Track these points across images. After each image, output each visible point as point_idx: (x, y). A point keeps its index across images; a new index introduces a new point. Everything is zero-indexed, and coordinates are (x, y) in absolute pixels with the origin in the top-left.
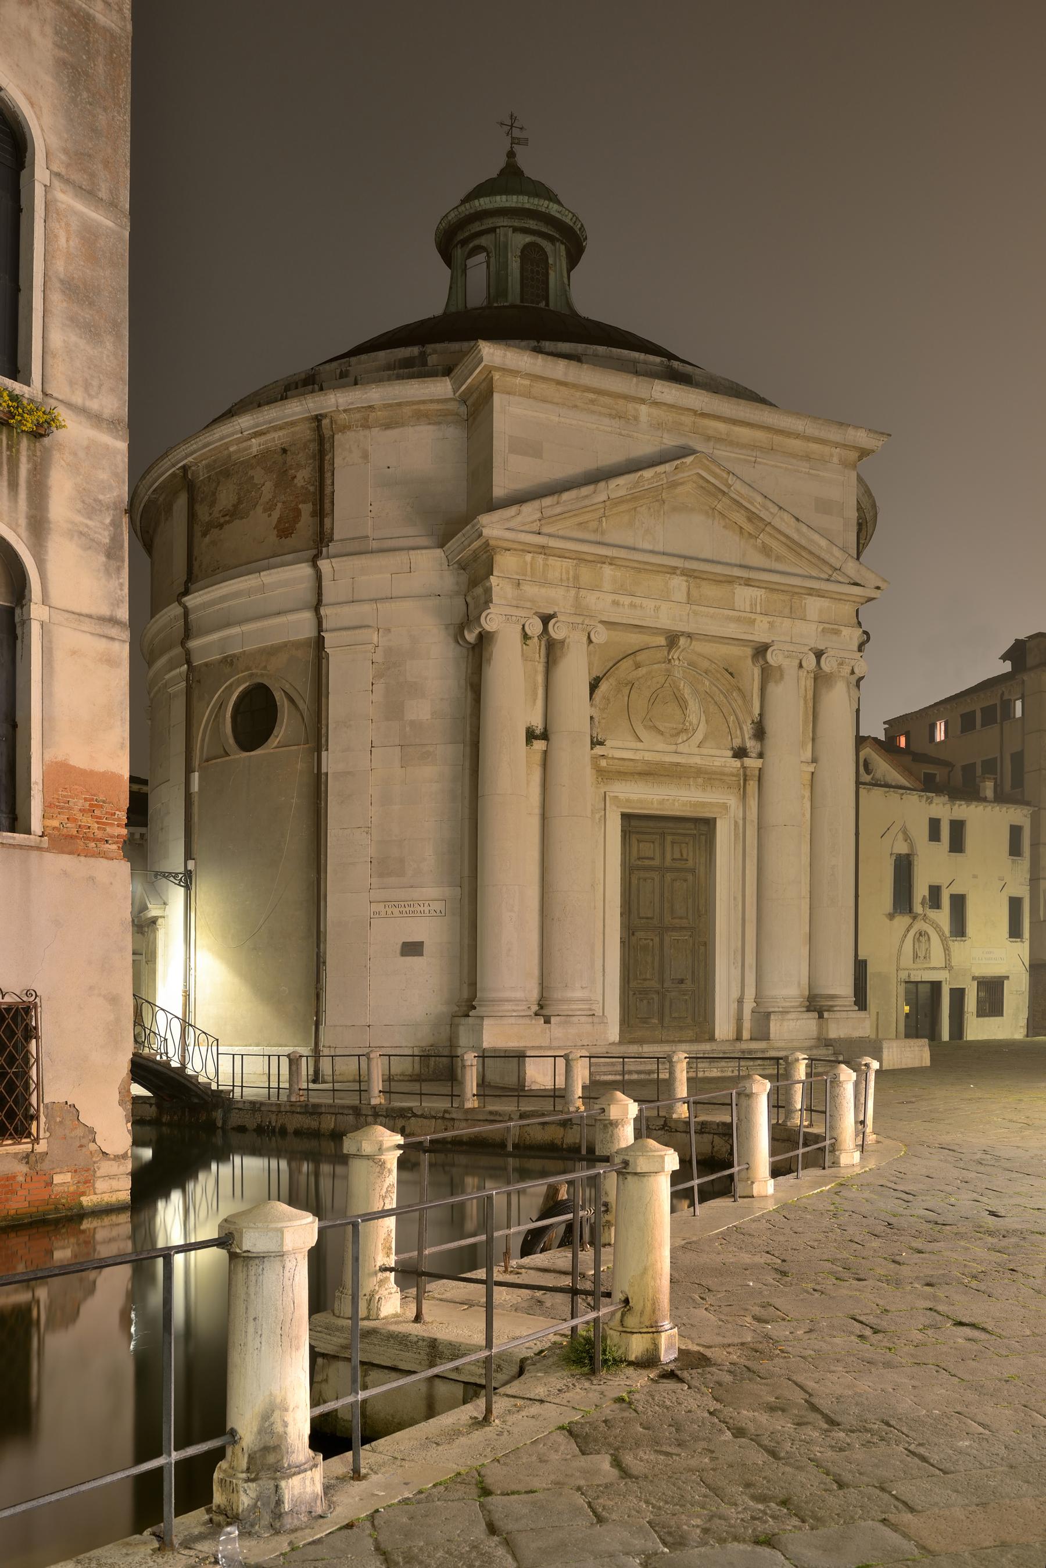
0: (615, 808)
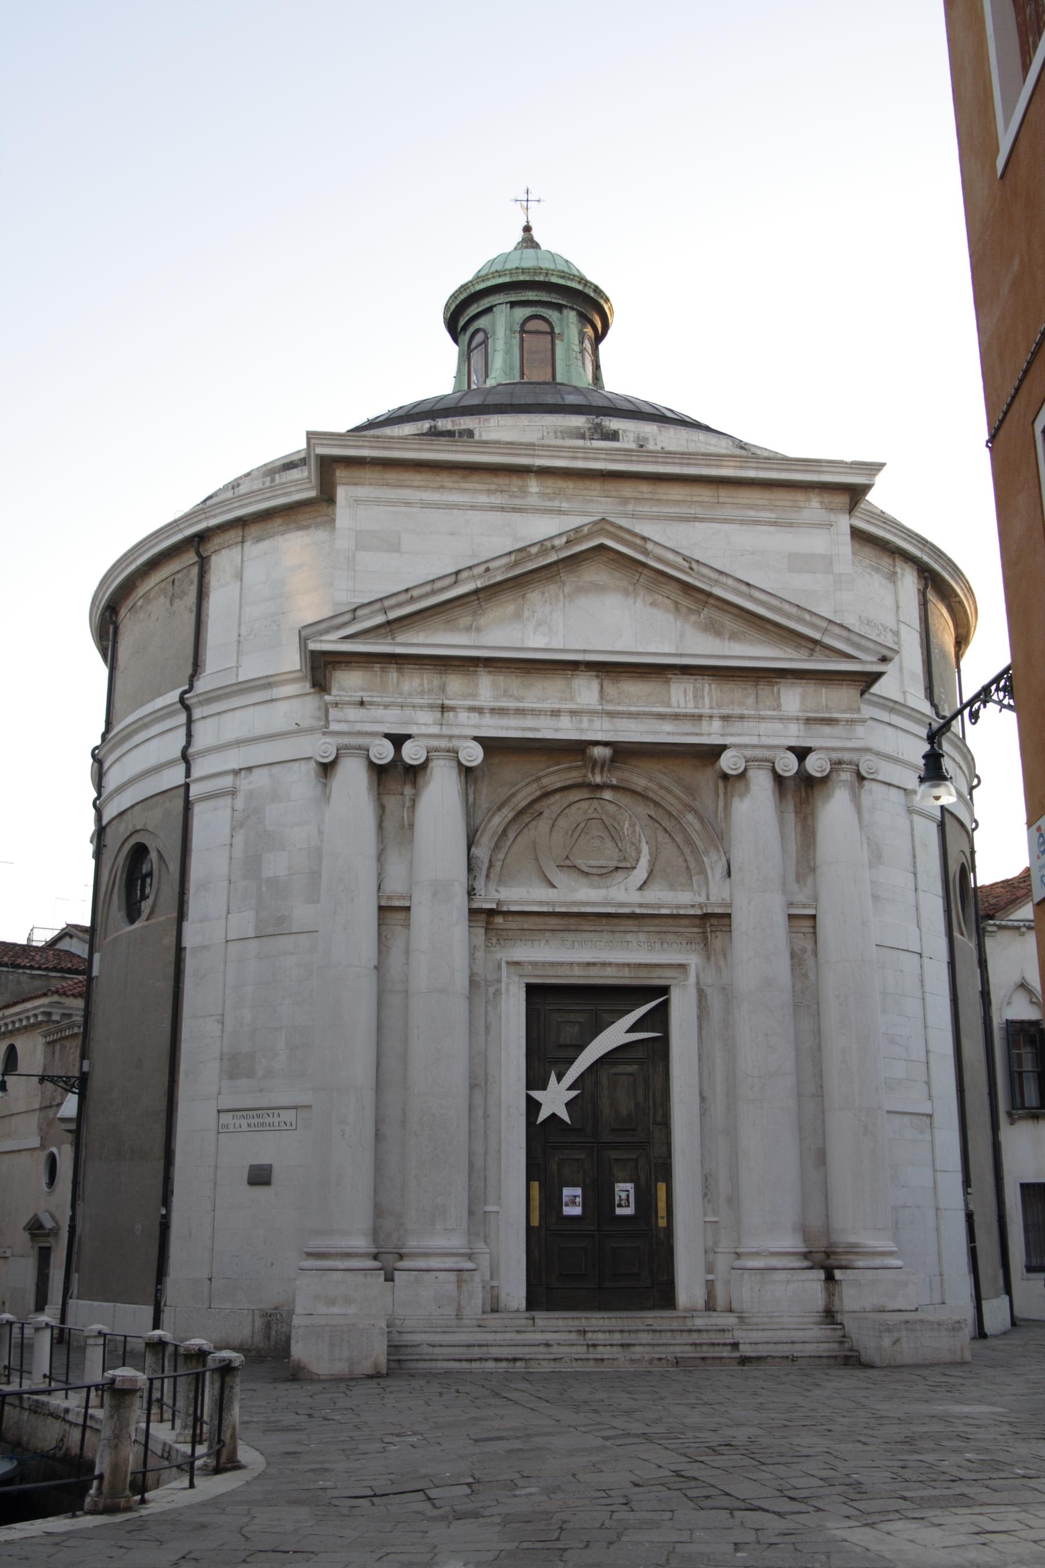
0: (517, 979)
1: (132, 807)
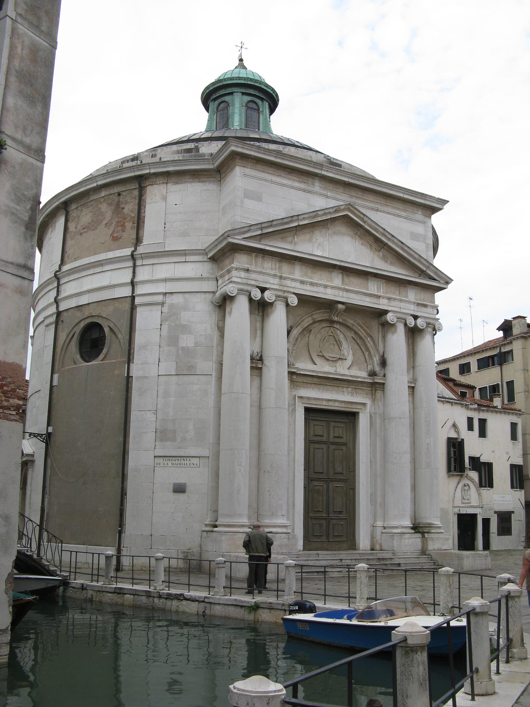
0: (301, 404)
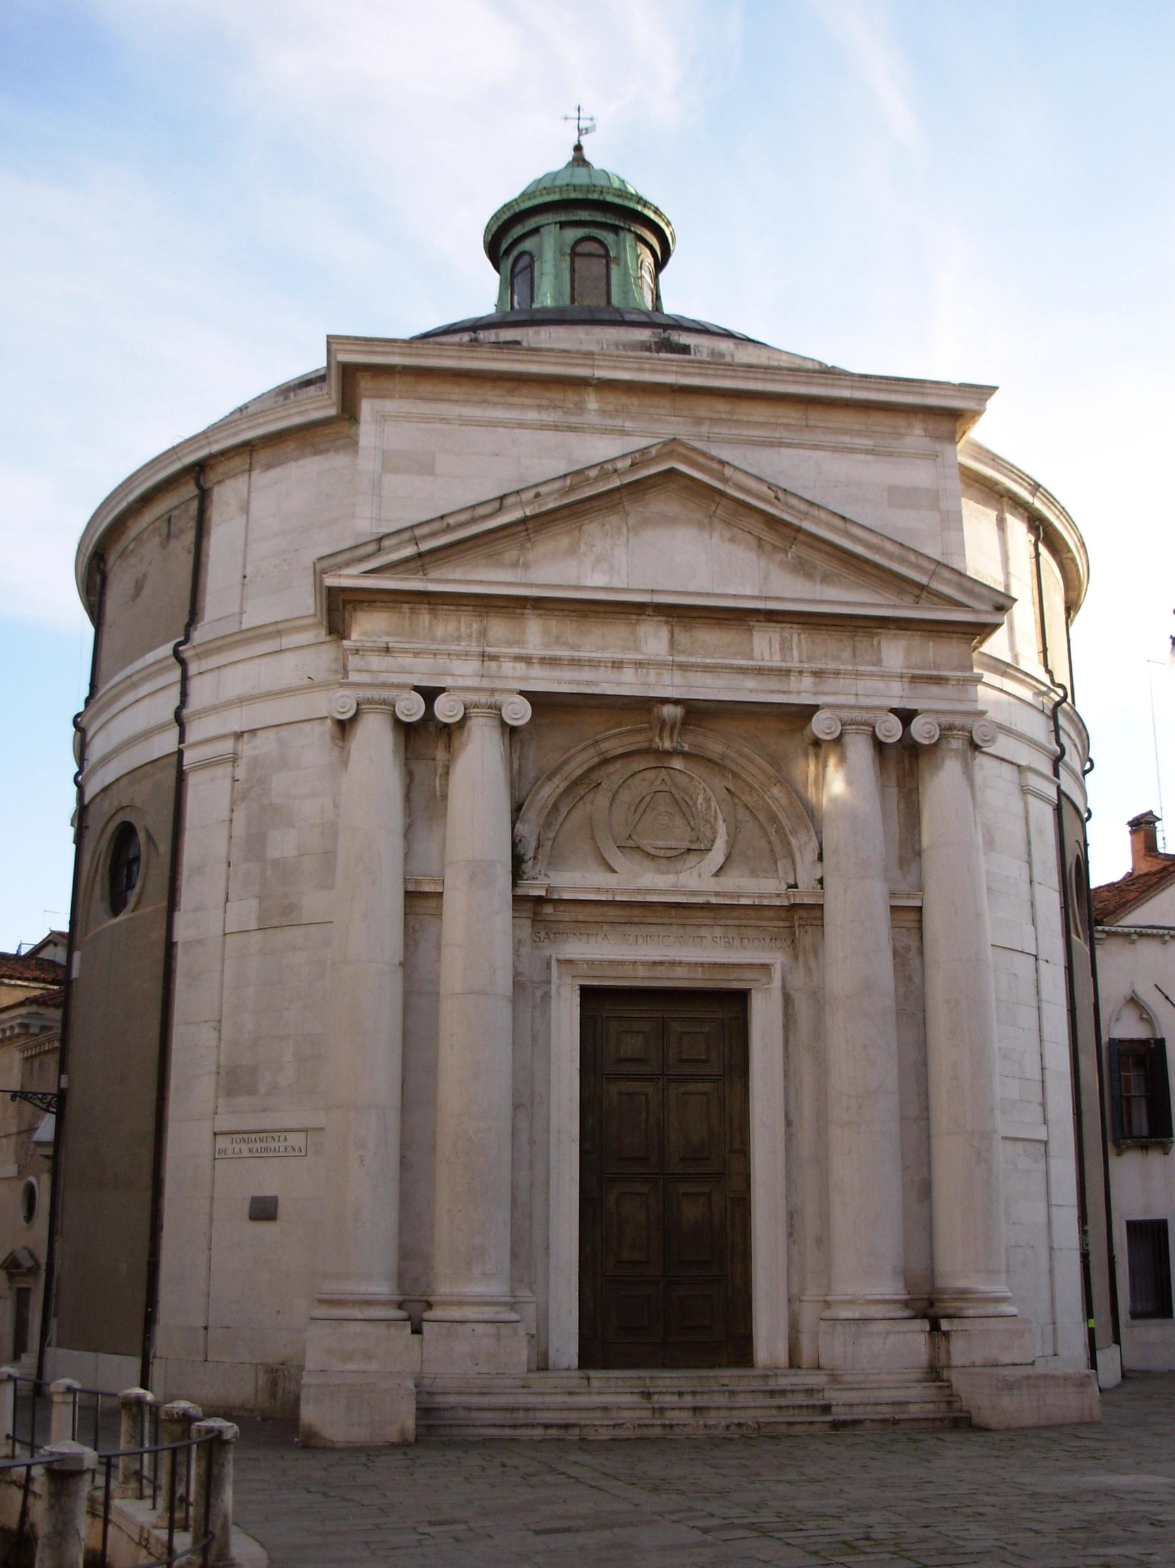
0: (569, 980)
1: (118, 780)
